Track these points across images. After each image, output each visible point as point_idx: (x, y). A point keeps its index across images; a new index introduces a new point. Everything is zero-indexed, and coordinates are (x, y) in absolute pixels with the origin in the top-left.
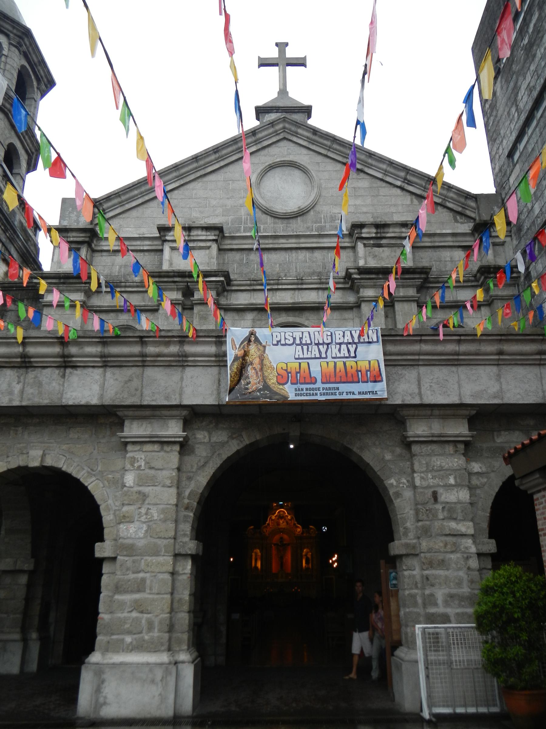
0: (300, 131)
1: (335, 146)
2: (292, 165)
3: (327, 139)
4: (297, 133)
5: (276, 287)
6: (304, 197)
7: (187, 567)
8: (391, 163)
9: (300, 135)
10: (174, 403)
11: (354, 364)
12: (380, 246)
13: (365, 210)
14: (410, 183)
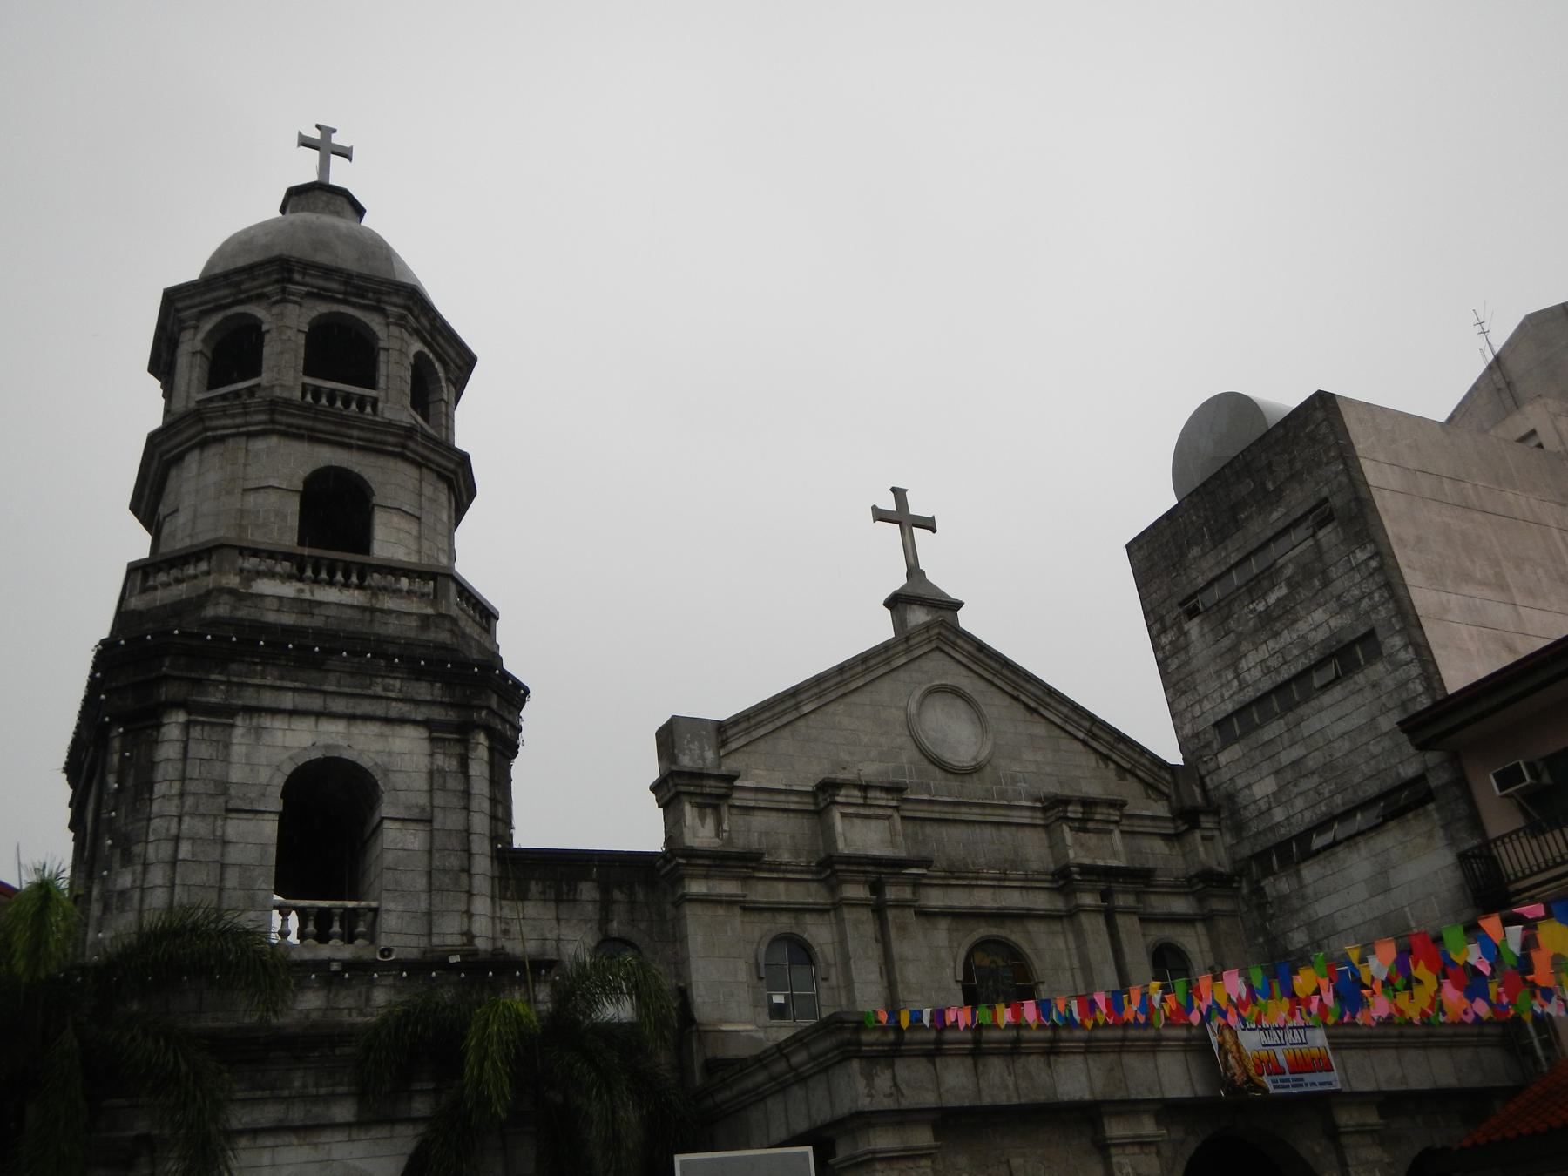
0: (960, 642)
1: (1005, 672)
2: (955, 692)
3: (996, 661)
4: (956, 644)
5: (973, 883)
6: (975, 743)
8: (1076, 708)
9: (958, 647)
10: (1157, 1096)
11: (1307, 1051)
12: (1086, 830)
13: (1048, 769)
14: (1095, 737)
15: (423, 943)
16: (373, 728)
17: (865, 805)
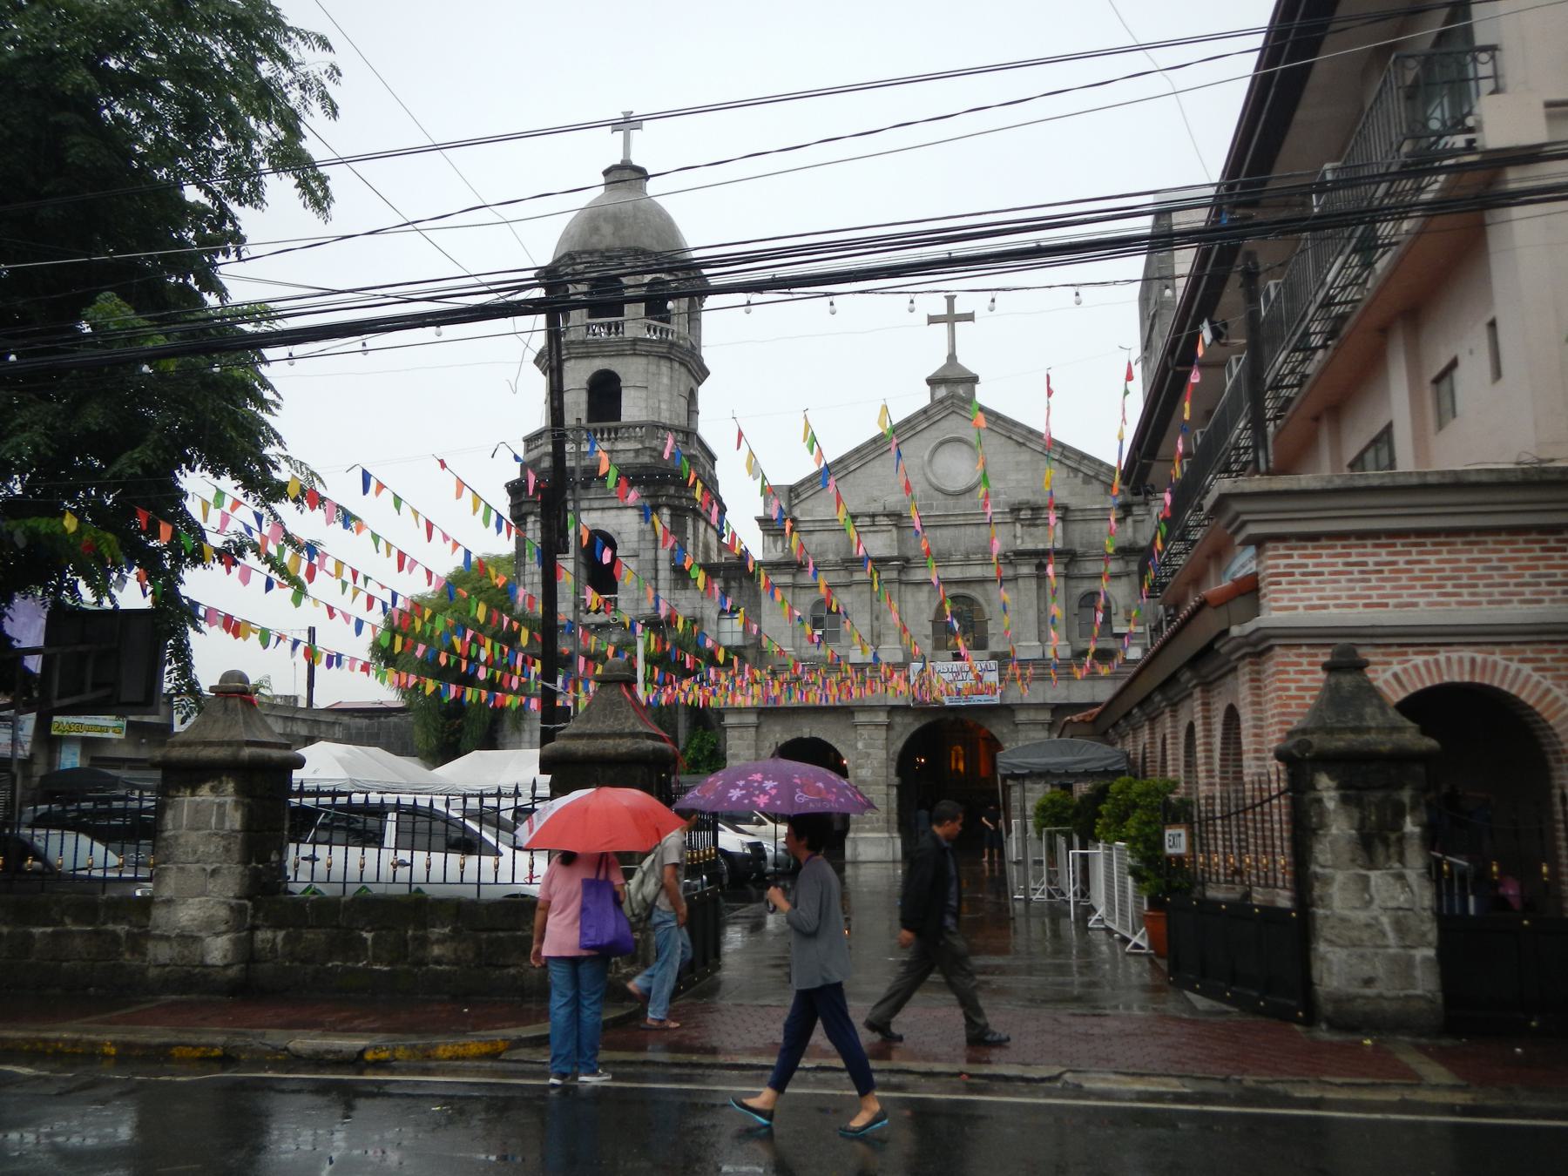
7: (894, 791)
12: (1036, 526)
13: (1025, 484)
14: (1066, 457)
15: (636, 613)
16: (613, 513)
17: (874, 525)
